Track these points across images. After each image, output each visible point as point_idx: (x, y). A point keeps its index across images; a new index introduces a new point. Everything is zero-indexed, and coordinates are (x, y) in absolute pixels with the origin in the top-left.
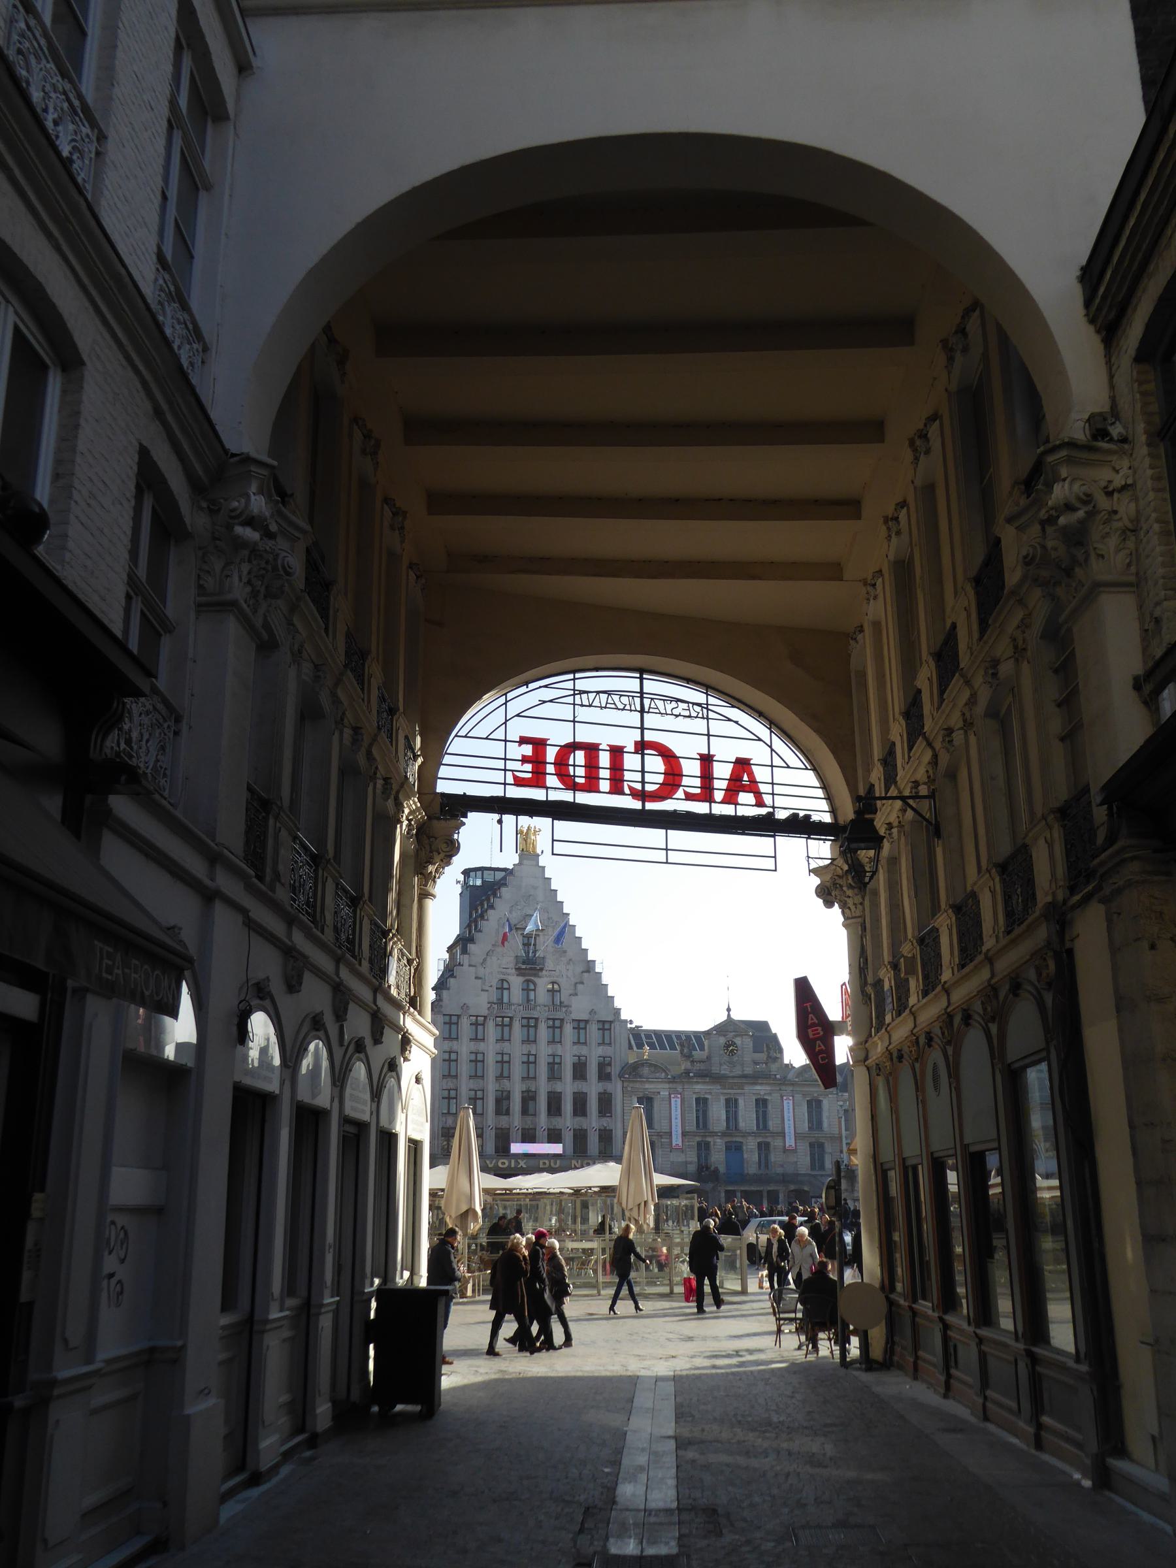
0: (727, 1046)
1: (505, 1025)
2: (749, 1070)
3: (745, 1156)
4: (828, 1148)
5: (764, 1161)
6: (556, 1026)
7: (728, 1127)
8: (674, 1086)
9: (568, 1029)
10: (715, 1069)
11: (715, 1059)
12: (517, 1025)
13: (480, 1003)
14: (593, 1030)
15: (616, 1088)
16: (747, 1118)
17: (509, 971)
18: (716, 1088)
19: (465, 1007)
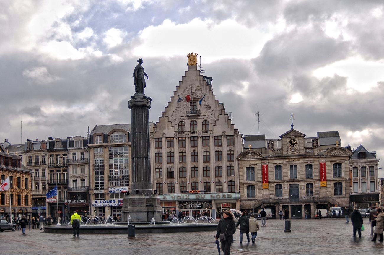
0: (291, 142)
1: (182, 141)
2: (302, 152)
3: (300, 190)
4: (344, 184)
5: (310, 192)
6: (206, 139)
7: (291, 178)
8: (263, 161)
9: (212, 140)
10: (285, 153)
11: (285, 148)
12: (188, 141)
13: (170, 132)
14: (224, 141)
15: (236, 164)
16: (301, 173)
17: (184, 118)
18: (285, 161)
19: (164, 134)
